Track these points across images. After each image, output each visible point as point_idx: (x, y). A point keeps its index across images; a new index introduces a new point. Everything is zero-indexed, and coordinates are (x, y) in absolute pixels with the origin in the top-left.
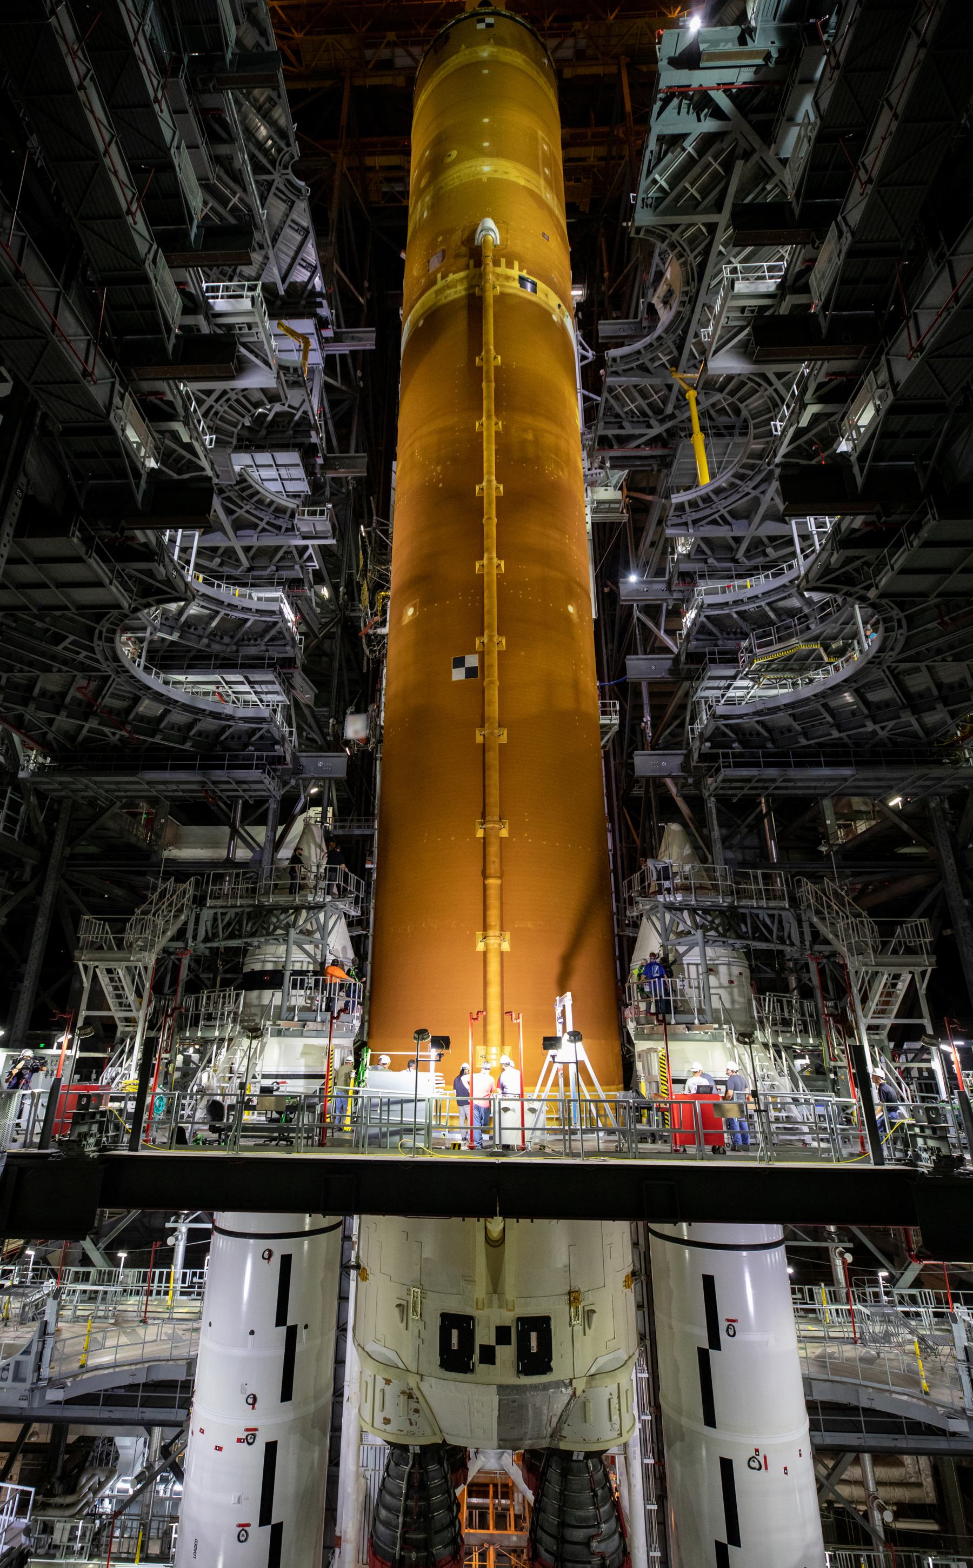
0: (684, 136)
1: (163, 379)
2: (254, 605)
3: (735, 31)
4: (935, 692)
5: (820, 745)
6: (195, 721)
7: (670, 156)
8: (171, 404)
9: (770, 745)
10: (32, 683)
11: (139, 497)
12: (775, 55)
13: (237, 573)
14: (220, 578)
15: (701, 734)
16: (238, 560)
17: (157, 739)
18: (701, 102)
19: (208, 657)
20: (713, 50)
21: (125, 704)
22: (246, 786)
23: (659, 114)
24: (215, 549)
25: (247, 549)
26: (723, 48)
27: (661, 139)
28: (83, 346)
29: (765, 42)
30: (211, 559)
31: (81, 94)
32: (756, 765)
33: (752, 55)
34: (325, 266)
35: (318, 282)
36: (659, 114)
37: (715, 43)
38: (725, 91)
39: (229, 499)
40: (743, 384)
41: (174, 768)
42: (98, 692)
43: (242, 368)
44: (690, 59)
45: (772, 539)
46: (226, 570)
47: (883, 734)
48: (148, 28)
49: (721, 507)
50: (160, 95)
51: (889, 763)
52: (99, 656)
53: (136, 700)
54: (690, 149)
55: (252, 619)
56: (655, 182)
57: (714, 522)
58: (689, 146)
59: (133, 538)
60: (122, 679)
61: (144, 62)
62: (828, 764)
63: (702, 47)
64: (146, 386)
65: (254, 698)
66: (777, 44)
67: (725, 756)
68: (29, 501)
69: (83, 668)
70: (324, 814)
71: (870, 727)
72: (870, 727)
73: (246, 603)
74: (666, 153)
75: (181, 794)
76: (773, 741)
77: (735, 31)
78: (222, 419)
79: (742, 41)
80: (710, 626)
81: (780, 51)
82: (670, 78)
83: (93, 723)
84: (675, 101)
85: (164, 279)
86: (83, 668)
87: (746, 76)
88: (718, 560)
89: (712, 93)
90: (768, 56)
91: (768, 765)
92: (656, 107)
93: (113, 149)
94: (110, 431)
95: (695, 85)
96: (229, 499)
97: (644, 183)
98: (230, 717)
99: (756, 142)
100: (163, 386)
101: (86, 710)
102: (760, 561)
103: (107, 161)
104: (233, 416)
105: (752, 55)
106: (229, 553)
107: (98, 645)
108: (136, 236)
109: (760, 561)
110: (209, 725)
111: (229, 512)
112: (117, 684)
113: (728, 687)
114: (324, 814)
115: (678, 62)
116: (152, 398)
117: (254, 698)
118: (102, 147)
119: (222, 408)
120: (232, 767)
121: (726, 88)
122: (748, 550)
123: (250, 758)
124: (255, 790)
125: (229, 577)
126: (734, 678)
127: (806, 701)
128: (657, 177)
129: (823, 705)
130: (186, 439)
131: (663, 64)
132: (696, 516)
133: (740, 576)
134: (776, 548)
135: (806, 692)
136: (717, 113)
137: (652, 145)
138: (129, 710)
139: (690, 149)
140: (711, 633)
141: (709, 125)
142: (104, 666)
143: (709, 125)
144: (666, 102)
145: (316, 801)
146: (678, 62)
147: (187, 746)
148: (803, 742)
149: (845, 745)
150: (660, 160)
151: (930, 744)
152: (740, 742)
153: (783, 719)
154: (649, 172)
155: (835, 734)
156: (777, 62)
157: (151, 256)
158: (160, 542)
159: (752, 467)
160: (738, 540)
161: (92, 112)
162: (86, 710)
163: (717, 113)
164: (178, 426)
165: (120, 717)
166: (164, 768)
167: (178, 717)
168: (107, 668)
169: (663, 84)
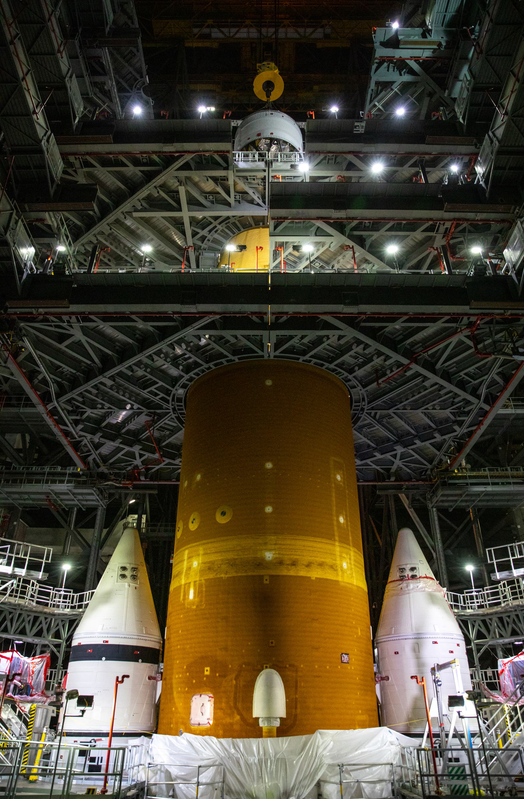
0: (393, 83)
1: (45, 211)
3: (419, 30)
7: (383, 92)
8: (49, 226)
12: (444, 44)
18: (401, 65)
20: (407, 39)
22: (80, 497)
23: (375, 71)
26: (412, 38)
27: (377, 83)
29: (437, 36)
31: (12, 47)
33: (430, 43)
36: (375, 71)
37: (409, 36)
38: (415, 61)
44: (394, 42)
50: (62, 49)
54: (396, 90)
56: (375, 106)
58: (396, 88)
61: (54, 31)
63: (400, 37)
64: (34, 215)
66: (445, 38)
70: (139, 520)
74: (381, 91)
75: (31, 502)
77: (419, 30)
79: (424, 35)
81: (447, 42)
82: (381, 52)
84: (386, 64)
87: (427, 54)
89: (407, 61)
90: (440, 45)
92: (374, 67)
93: (29, 78)
95: (397, 56)
97: (368, 107)
99: (437, 88)
103: (24, 84)
105: (430, 43)
108: (37, 127)
114: (139, 520)
115: (386, 44)
116: (39, 224)
118: (21, 75)
121: (416, 59)
124: (87, 500)
128: (376, 103)
131: (377, 45)
136: (411, 71)
137: (372, 86)
139: (396, 90)
141: (407, 78)
143: (407, 78)
144: (380, 64)
145: (133, 510)
146: (386, 44)
150: (377, 94)
154: (371, 101)
156: (446, 47)
157: (45, 138)
161: (18, 56)
163: (411, 71)
169: (377, 55)
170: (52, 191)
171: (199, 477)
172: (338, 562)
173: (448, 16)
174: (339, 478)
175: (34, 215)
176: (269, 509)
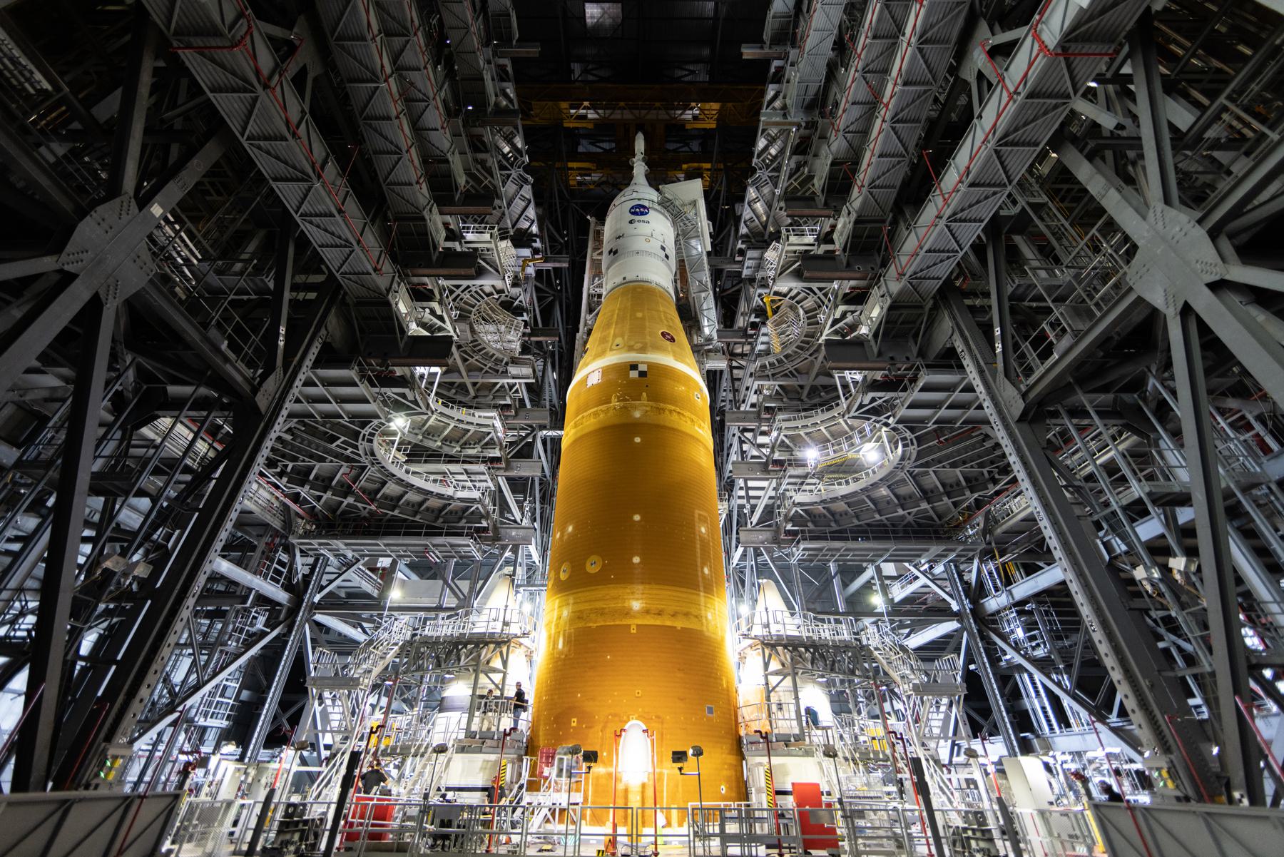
2: (476, 420)
4: (941, 489)
5: (868, 525)
6: (426, 500)
8: (431, 291)
9: (833, 524)
10: (311, 469)
11: (402, 346)
13: (463, 399)
14: (454, 402)
15: (786, 516)
16: (467, 391)
17: (396, 513)
19: (440, 456)
21: (377, 485)
24: (452, 384)
25: (474, 384)
26: (774, 119)
28: (377, 254)
30: (449, 390)
32: (825, 539)
34: (541, 220)
35: (535, 229)
39: (465, 352)
40: (798, 294)
41: (406, 534)
42: (356, 479)
43: (480, 273)
45: (824, 387)
46: (459, 398)
47: (910, 518)
48: (443, 94)
49: (789, 366)
51: (917, 538)
52: (361, 452)
53: (384, 483)
55: (472, 429)
57: (786, 375)
59: (393, 372)
60: (377, 467)
62: (875, 538)
64: (415, 280)
65: (469, 484)
67: (803, 532)
68: (326, 347)
69: (348, 459)
71: (901, 512)
72: (901, 512)
73: (470, 419)
76: (836, 521)
78: (466, 303)
80: (787, 441)
83: (350, 500)
85: (437, 222)
86: (348, 459)
88: (790, 399)
91: (833, 539)
94: (388, 304)
96: (465, 352)
98: (451, 498)
100: (426, 280)
101: (346, 490)
102: (817, 400)
104: (473, 301)
106: (462, 388)
107: (363, 445)
109: (817, 400)
110: (434, 503)
111: (465, 360)
112: (372, 472)
113: (802, 484)
117: (469, 484)
119: (466, 296)
120: (448, 534)
122: (809, 394)
123: (463, 528)
125: (460, 402)
126: (806, 477)
127: (855, 494)
129: (868, 497)
130: (439, 313)
132: (773, 371)
133: (805, 410)
134: (827, 393)
135: (853, 487)
138: (379, 490)
140: (788, 447)
142: (363, 459)
147: (417, 518)
148: (856, 522)
149: (885, 525)
151: (942, 526)
152: (813, 522)
153: (842, 506)
155: (877, 517)
158: (413, 375)
159: (808, 343)
160: (801, 387)
162: (346, 490)
164: (435, 305)
165: (372, 495)
166: (398, 534)
167: (412, 497)
168: (365, 461)
170: (434, 258)
171: (570, 529)
172: (703, 613)
173: (808, 99)
174: (703, 530)
175: (415, 280)
176: (636, 560)
